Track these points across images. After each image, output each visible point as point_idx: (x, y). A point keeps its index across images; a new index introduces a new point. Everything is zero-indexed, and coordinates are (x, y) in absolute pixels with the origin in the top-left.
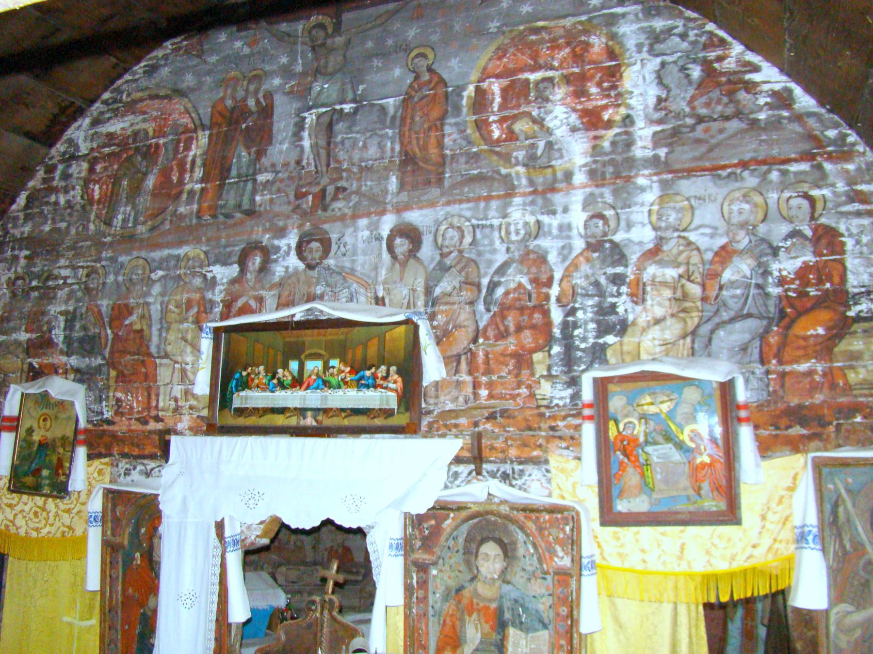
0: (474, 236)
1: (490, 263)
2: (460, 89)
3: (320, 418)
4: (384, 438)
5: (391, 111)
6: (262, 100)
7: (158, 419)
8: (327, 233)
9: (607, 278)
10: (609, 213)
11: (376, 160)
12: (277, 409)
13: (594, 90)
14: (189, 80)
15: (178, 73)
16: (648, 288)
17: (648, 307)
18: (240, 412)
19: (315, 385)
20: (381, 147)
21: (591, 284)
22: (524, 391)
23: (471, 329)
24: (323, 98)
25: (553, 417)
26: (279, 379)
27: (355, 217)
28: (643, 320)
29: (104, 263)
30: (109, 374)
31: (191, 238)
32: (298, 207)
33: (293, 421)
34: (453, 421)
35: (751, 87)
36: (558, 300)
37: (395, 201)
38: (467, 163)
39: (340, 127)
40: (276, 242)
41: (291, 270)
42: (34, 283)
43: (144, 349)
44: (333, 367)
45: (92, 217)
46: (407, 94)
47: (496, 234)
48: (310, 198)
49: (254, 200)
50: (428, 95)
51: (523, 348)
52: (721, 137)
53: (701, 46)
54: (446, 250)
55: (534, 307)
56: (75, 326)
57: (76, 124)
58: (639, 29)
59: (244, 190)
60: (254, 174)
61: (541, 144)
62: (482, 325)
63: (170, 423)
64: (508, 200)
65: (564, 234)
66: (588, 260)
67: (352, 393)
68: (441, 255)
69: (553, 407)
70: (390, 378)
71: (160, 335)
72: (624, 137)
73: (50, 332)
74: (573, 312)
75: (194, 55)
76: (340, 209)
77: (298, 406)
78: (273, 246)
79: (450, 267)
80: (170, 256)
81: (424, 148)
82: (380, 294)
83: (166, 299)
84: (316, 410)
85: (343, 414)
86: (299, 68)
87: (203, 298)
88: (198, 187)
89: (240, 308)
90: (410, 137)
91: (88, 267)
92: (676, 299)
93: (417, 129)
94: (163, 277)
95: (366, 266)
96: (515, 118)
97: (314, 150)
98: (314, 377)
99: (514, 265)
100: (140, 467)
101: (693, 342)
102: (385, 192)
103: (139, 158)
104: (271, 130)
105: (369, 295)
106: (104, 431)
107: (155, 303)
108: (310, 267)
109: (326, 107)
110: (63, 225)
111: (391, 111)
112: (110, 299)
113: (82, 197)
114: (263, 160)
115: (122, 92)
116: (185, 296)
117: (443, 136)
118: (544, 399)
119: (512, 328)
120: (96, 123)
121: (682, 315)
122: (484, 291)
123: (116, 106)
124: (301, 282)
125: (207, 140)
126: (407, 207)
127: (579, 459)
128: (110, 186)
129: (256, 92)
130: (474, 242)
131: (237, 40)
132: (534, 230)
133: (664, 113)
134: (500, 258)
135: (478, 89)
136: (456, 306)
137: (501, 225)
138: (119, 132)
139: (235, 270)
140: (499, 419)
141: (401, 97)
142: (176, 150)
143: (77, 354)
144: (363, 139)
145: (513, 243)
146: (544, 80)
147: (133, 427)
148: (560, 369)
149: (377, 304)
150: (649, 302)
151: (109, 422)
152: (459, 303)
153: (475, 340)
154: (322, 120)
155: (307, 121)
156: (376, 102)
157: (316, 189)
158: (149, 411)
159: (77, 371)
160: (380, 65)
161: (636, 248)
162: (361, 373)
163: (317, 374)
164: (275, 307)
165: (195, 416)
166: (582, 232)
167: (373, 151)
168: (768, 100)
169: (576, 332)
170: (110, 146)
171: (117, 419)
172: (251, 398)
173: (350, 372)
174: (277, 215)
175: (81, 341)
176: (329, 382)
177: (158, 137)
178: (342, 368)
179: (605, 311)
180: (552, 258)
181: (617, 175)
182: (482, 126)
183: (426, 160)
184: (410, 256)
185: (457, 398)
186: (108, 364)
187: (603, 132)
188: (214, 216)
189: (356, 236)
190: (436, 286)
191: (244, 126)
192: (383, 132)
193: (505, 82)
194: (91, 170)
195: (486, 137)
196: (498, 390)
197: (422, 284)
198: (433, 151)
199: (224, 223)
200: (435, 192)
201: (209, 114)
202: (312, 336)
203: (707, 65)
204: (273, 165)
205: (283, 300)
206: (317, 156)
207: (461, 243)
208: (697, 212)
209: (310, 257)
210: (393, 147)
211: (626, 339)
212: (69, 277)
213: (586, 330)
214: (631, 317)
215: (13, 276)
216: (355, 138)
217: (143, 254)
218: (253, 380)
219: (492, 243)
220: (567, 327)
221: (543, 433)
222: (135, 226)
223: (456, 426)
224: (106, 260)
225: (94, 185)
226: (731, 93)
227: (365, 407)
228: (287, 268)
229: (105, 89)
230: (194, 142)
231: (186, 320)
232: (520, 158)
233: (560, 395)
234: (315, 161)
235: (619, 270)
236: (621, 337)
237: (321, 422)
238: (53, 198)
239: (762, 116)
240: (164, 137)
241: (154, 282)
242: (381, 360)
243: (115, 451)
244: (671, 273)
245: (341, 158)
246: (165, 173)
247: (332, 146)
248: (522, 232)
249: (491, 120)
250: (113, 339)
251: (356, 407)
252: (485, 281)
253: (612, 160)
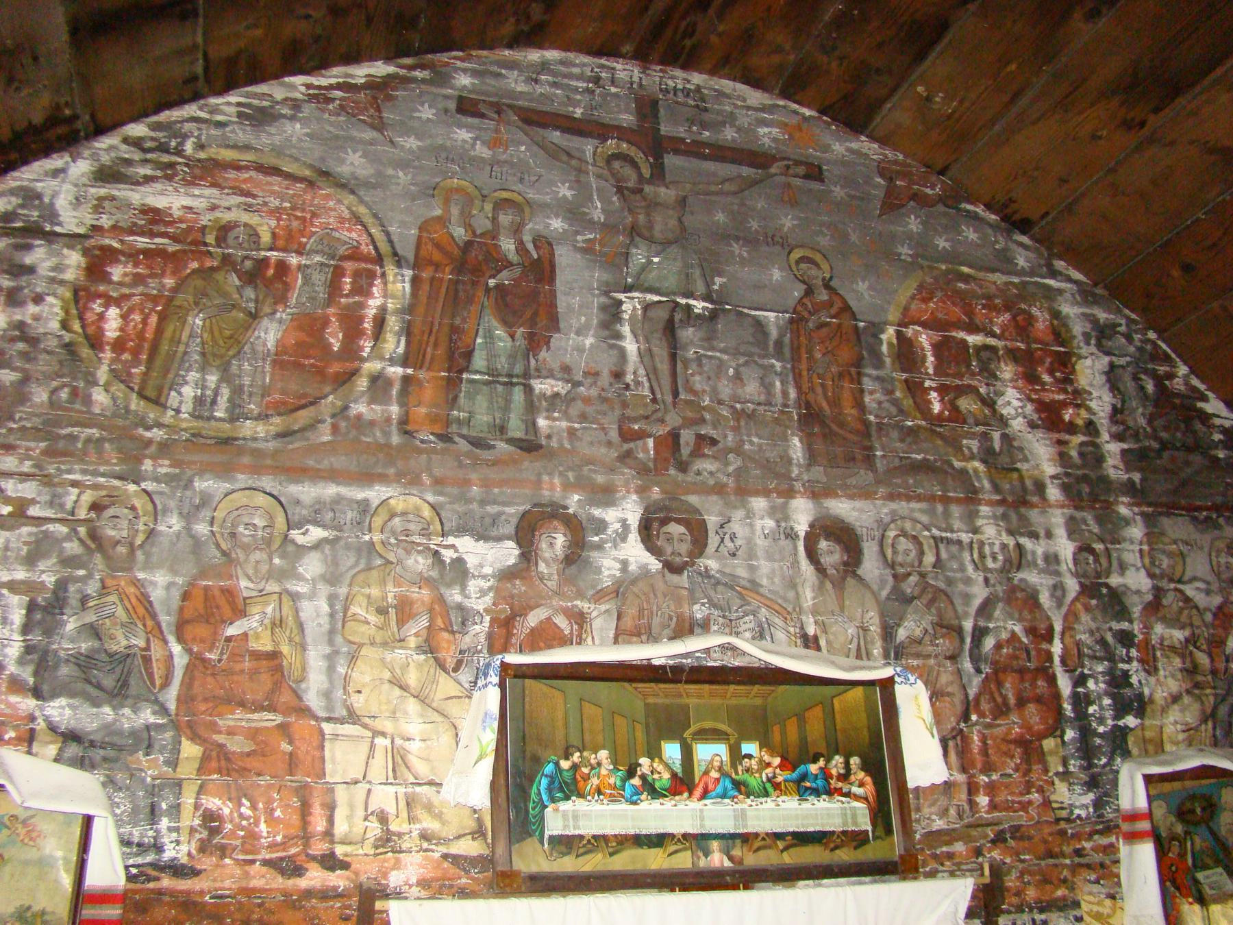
0: (938, 555)
1: (967, 598)
2: (876, 329)
3: (737, 852)
4: (838, 885)
5: (774, 333)
6: (530, 246)
7: (330, 862)
8: (697, 511)
9: (1114, 636)
10: (1099, 547)
11: (759, 404)
12: (648, 836)
13: (1046, 378)
14: (353, 163)
15: (338, 143)
16: (1158, 654)
17: (1162, 679)
18: (566, 843)
19: (719, 789)
20: (767, 387)
21: (1097, 642)
22: (1035, 796)
23: (958, 699)
24: (651, 277)
25: (1077, 836)
26: (643, 777)
27: (744, 493)
28: (1160, 695)
29: (149, 485)
30: (176, 749)
31: (392, 471)
32: (628, 454)
33: (683, 861)
34: (944, 849)
35: (1205, 417)
36: (1063, 662)
37: (806, 478)
38: (902, 440)
39: (687, 333)
40: (597, 512)
41: (632, 567)
43: (285, 698)
44: (749, 756)
45: (103, 374)
46: (795, 312)
47: (966, 556)
48: (650, 442)
49: (534, 424)
50: (827, 324)
51: (1029, 729)
52: (1189, 470)
53: (1147, 357)
54: (901, 570)
55: (1037, 670)
56: (63, 624)
57: (56, 162)
58: (1083, 314)
59: (508, 402)
60: (526, 375)
61: (996, 436)
62: (972, 692)
63: (367, 869)
64: (972, 507)
65: (1052, 568)
66: (1087, 609)
67: (790, 804)
68: (895, 576)
69: (1074, 821)
70: (852, 778)
71: (331, 669)
72: (1090, 449)
74: (1081, 681)
75: (364, 121)
76: (711, 473)
77: (691, 831)
78: (592, 519)
79: (913, 598)
80: (338, 500)
81: (835, 403)
82: (811, 630)
83: (343, 591)
84: (728, 839)
85: (781, 845)
86: (598, 215)
87: (441, 600)
88: (396, 371)
89: (533, 630)
90: (810, 380)
91: (96, 487)
92: (1187, 671)
93: (821, 371)
95: (776, 580)
96: (961, 391)
97: (646, 359)
98: (714, 774)
99: (1000, 605)
101: (1214, 728)
102: (789, 461)
103: (234, 280)
104: (553, 305)
105: (792, 630)
106: (160, 892)
107: (312, 596)
108: (672, 568)
109: (661, 295)
111: (774, 333)
112: (173, 571)
113: (65, 325)
114: (543, 354)
115: (185, 137)
116: (392, 593)
117: (862, 391)
118: (1062, 808)
119: (1012, 700)
120: (106, 175)
121: (1197, 692)
122: (968, 640)
123: (166, 158)
124: (659, 595)
125: (408, 286)
126: (829, 492)
127: (1112, 897)
128: (153, 320)
129: (517, 230)
130: (938, 563)
131: (460, 126)
132: (1014, 555)
133: (1122, 427)
134: (979, 593)
135: (899, 334)
136: (932, 661)
137: (972, 542)
138: (177, 213)
139: (509, 553)
140: (1012, 843)
141: (788, 315)
142: (334, 287)
143: (72, 695)
144: (734, 364)
145: (991, 571)
146: (986, 347)
147: (256, 883)
148: (1078, 763)
149: (807, 646)
150: (1162, 673)
151: (176, 870)
152: (936, 656)
153: (966, 718)
154: (651, 314)
155: (624, 307)
156: (746, 311)
157: (662, 430)
158: (307, 844)
159: (72, 736)
160: (745, 254)
161: (1136, 599)
162: (802, 768)
163: (720, 769)
164: (612, 634)
165: (437, 855)
166: (1071, 566)
167: (752, 389)
168: (1221, 437)
169: (1091, 710)
170: (152, 235)
171: (206, 862)
172: (587, 815)
173: (781, 766)
174: (590, 462)
175: (85, 663)
176: (745, 784)
177: (284, 250)
178: (767, 758)
179: (1118, 681)
180: (1045, 599)
181: (1094, 498)
182: (915, 389)
183: (842, 425)
184: (846, 571)
185: (947, 810)
186: (176, 725)
187: (1067, 437)
188: (445, 438)
189: (751, 525)
190: (899, 625)
191: (492, 282)
192: (766, 362)
193: (937, 336)
194: (97, 266)
195: (923, 408)
196: (1001, 797)
197: (876, 620)
198: (850, 411)
199: (468, 454)
200: (863, 476)
201: (413, 240)
202: (700, 696)
203: (1159, 380)
204: (566, 369)
205: (628, 622)
206: (652, 373)
207: (920, 562)
208: (1188, 560)
209: (669, 550)
210: (784, 391)
211: (1147, 722)
212: (33, 502)
213: (1101, 708)
214: (1146, 691)
216: (719, 359)
217: (267, 483)
218: (586, 778)
219: (962, 569)
220: (1081, 701)
221: (1068, 861)
222: (233, 419)
223: (950, 856)
224: (157, 479)
225: (107, 306)
226: (1188, 421)
227: (818, 828)
228: (625, 564)
229: (135, 119)
230: (378, 282)
232: (975, 450)
233: (1078, 801)
234: (649, 380)
235: (1125, 625)
236: (1142, 719)
237: (741, 862)
239: (1221, 455)
240: (299, 253)
241: (302, 550)
242: (834, 748)
244: (1178, 635)
245: (698, 387)
246: (311, 327)
247: (679, 366)
248: (1000, 558)
249: (927, 384)
250: (189, 669)
251: (802, 830)
252: (968, 625)
253: (1085, 476)
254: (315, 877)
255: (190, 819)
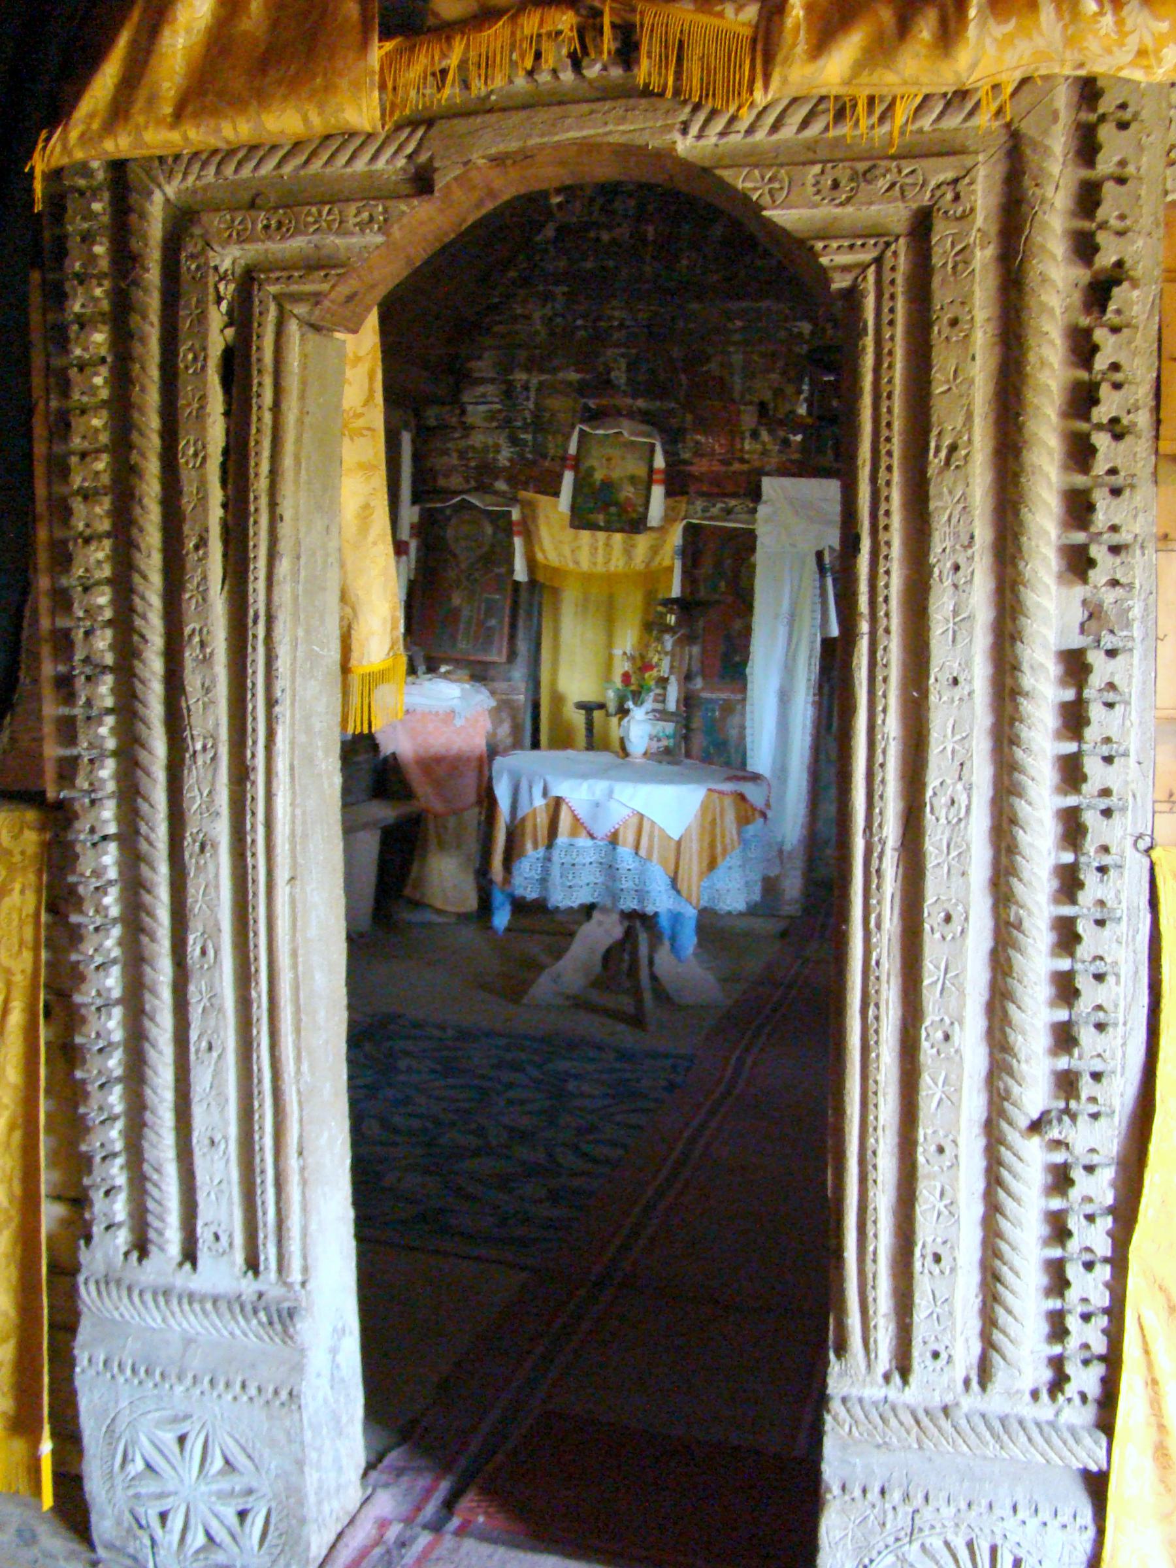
7: (742, 461)
42: (579, 322)
45: (648, 258)
73: (608, 373)
94: (743, 328)
100: (719, 505)
110: (611, 264)
215: (550, 313)
231: (772, 370)
238: (592, 234)
243: (692, 489)
254: (737, 466)
255: (691, 444)
